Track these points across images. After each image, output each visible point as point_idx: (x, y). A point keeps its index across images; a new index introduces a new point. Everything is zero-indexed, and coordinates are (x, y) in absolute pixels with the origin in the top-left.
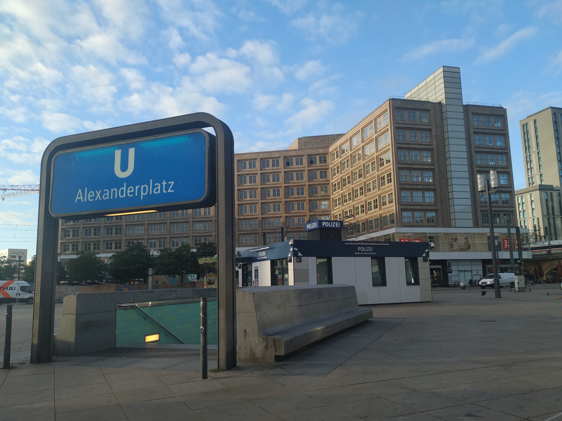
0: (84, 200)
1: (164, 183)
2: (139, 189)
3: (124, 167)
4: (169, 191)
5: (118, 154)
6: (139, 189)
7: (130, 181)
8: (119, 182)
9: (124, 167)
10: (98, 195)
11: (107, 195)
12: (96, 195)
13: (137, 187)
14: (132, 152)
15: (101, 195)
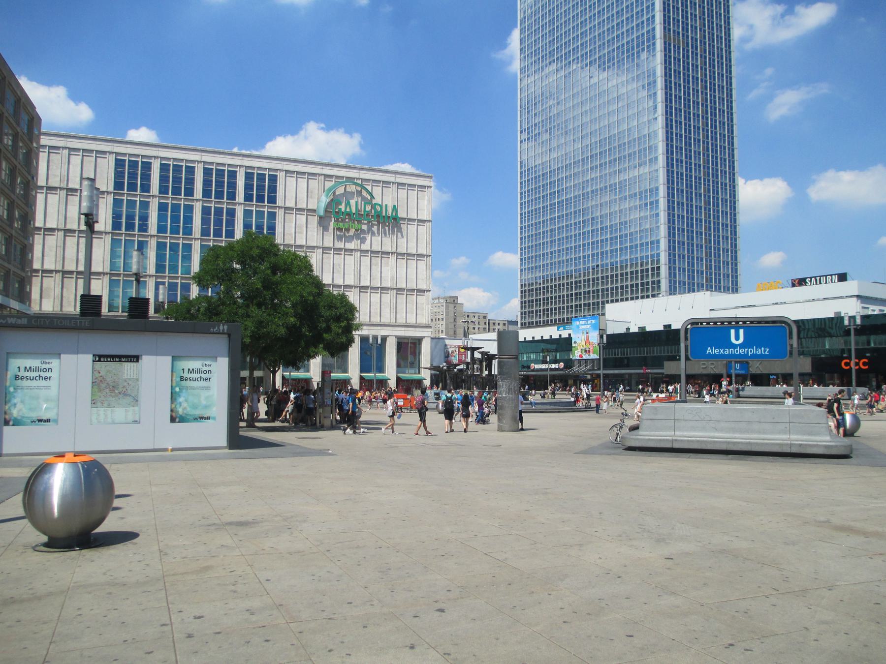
0: (712, 351)
1: (763, 349)
2: (748, 351)
3: (737, 338)
4: (766, 353)
5: (733, 332)
6: (748, 351)
7: (741, 346)
8: (735, 346)
9: (737, 338)
10: (722, 351)
11: (727, 352)
12: (720, 351)
13: (746, 350)
14: (741, 331)
15: (724, 351)
